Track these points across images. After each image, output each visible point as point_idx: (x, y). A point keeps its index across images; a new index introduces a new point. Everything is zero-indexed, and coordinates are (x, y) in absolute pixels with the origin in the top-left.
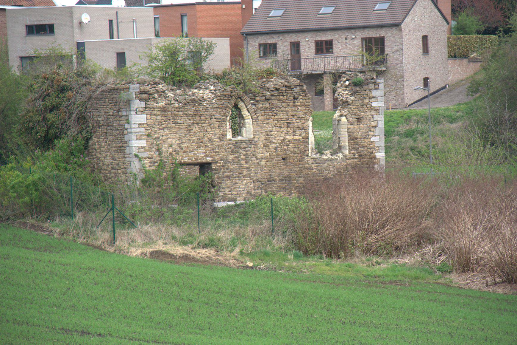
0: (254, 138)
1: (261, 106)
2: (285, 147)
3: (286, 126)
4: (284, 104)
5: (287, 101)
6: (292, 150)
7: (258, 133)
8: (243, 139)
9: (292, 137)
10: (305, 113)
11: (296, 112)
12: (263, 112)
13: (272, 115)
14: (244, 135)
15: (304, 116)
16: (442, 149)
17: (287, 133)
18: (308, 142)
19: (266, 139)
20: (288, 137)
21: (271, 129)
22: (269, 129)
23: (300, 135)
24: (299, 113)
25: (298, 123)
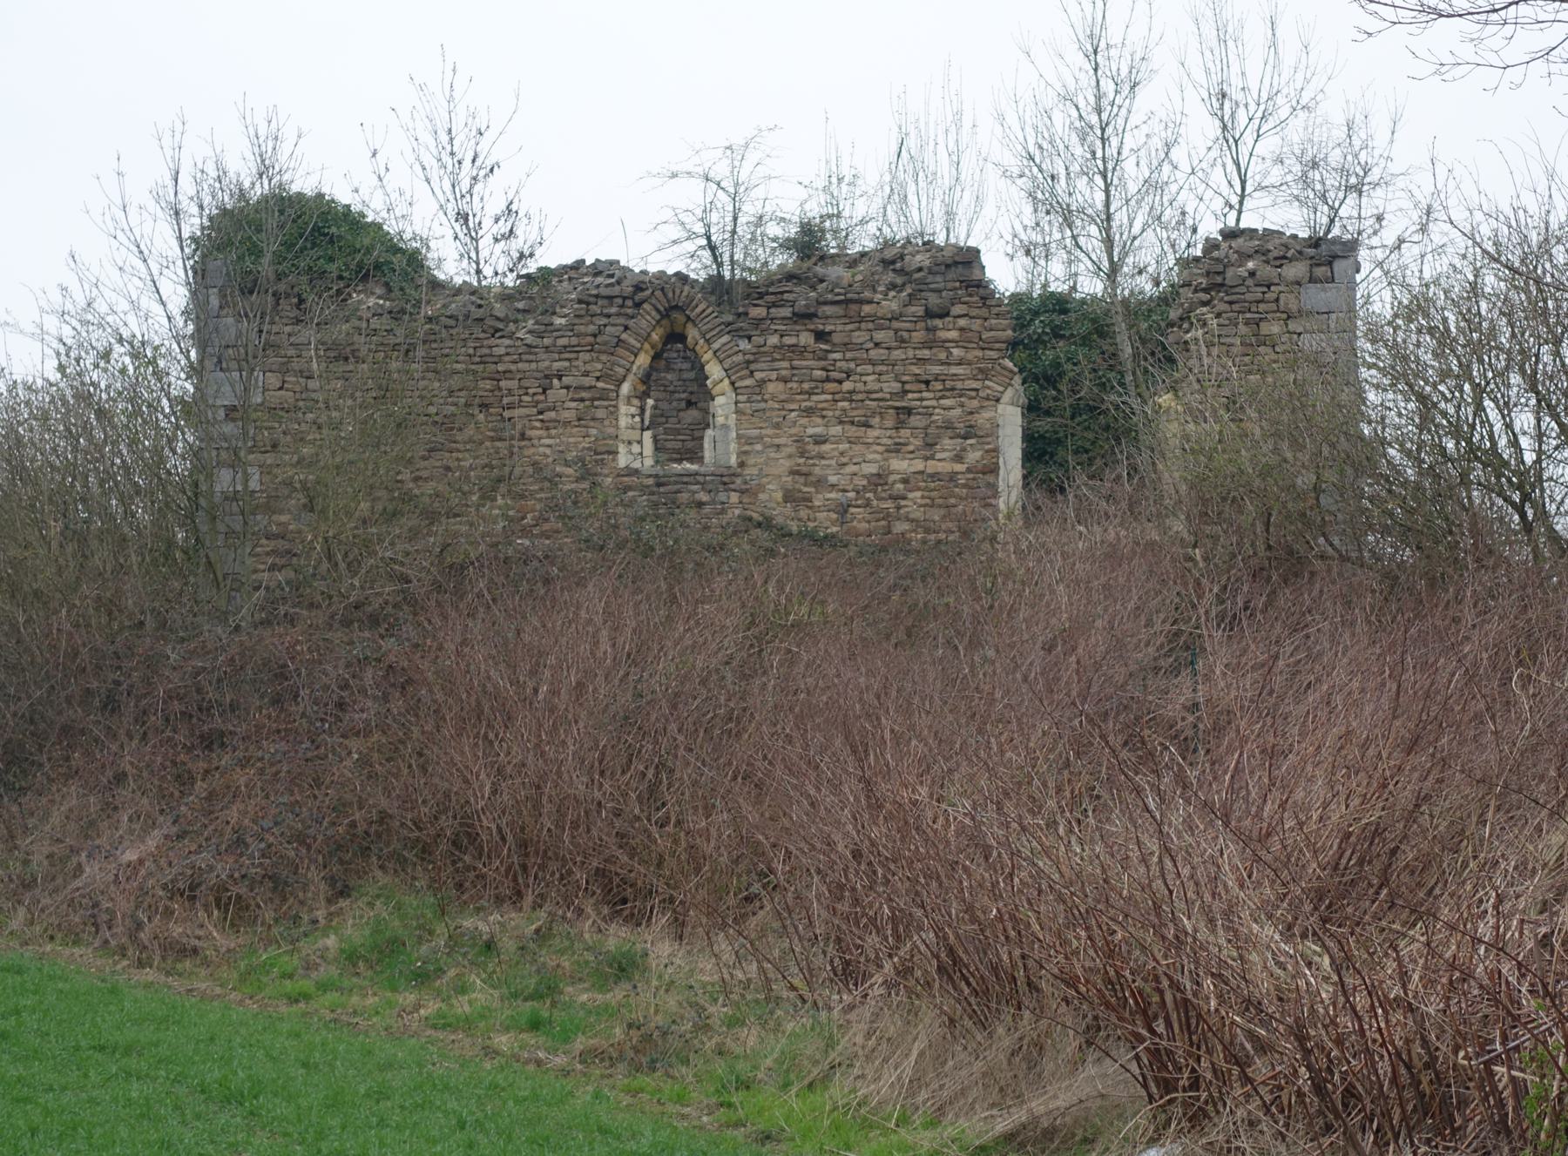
0: (742, 465)
1: (773, 340)
2: (889, 504)
3: (889, 423)
4: (879, 336)
5: (895, 324)
6: (918, 514)
7: (758, 447)
8: (703, 470)
9: (919, 465)
10: (985, 374)
11: (936, 369)
12: (785, 364)
13: (828, 380)
14: (708, 454)
15: (975, 385)
16: (1052, 455)
17: (897, 449)
18: (993, 487)
19: (793, 473)
20: (900, 465)
21: (818, 430)
22: (810, 431)
23: (959, 458)
24: (954, 370)
25: (951, 410)
